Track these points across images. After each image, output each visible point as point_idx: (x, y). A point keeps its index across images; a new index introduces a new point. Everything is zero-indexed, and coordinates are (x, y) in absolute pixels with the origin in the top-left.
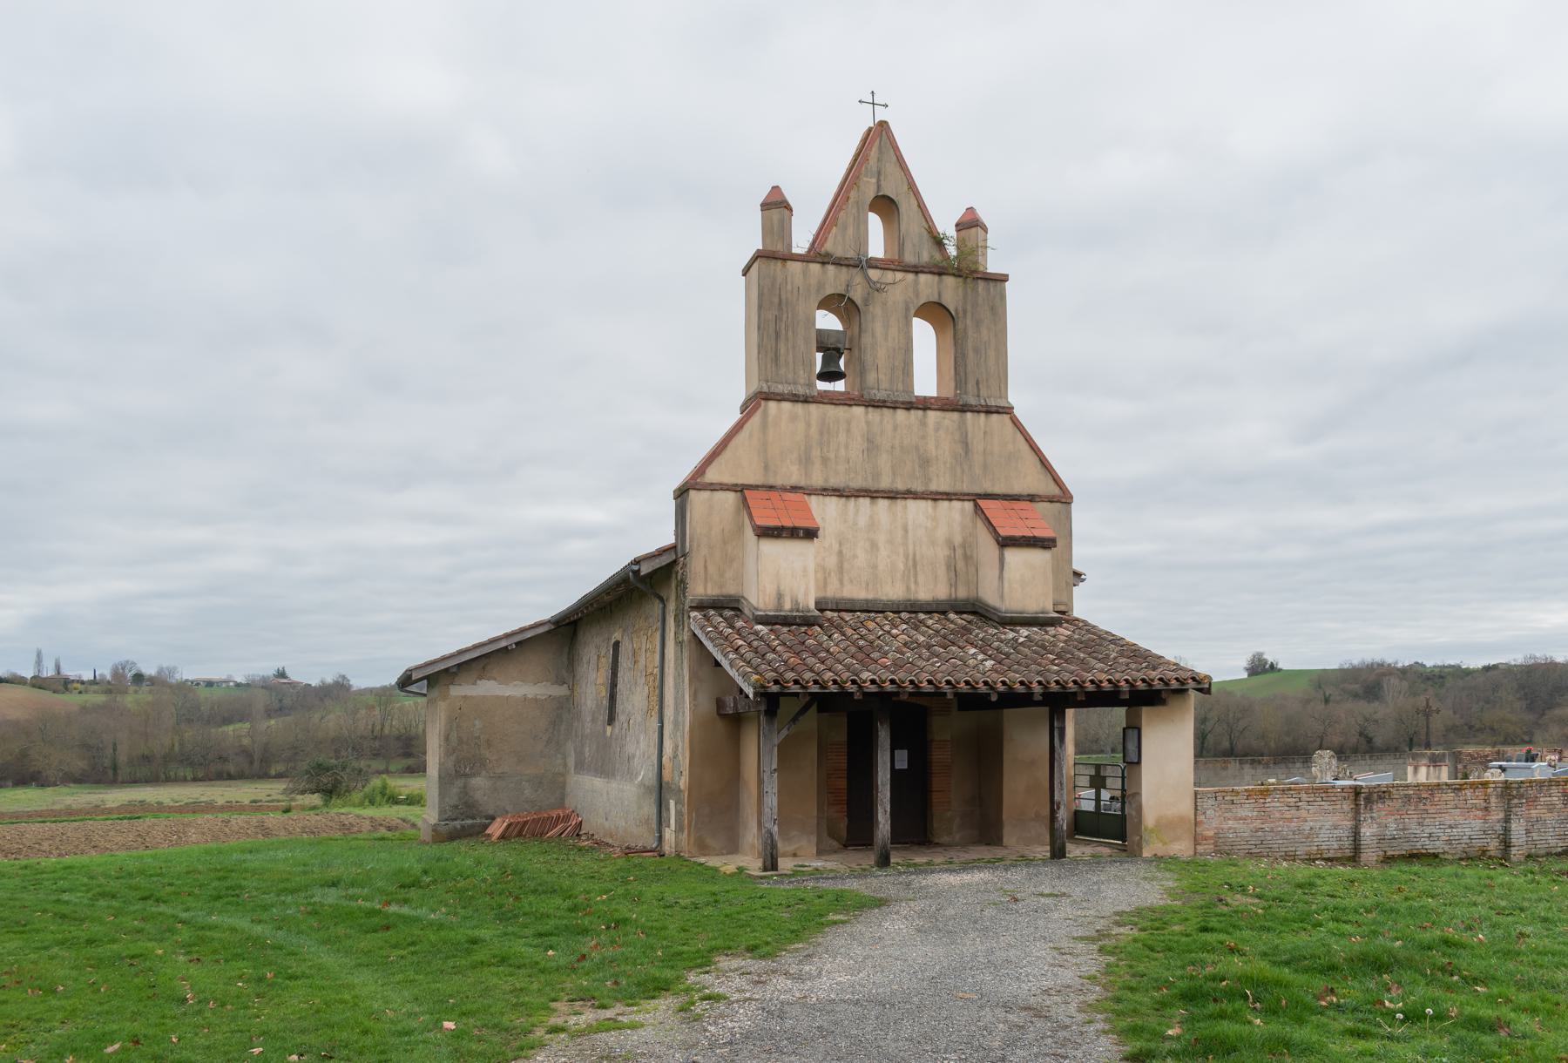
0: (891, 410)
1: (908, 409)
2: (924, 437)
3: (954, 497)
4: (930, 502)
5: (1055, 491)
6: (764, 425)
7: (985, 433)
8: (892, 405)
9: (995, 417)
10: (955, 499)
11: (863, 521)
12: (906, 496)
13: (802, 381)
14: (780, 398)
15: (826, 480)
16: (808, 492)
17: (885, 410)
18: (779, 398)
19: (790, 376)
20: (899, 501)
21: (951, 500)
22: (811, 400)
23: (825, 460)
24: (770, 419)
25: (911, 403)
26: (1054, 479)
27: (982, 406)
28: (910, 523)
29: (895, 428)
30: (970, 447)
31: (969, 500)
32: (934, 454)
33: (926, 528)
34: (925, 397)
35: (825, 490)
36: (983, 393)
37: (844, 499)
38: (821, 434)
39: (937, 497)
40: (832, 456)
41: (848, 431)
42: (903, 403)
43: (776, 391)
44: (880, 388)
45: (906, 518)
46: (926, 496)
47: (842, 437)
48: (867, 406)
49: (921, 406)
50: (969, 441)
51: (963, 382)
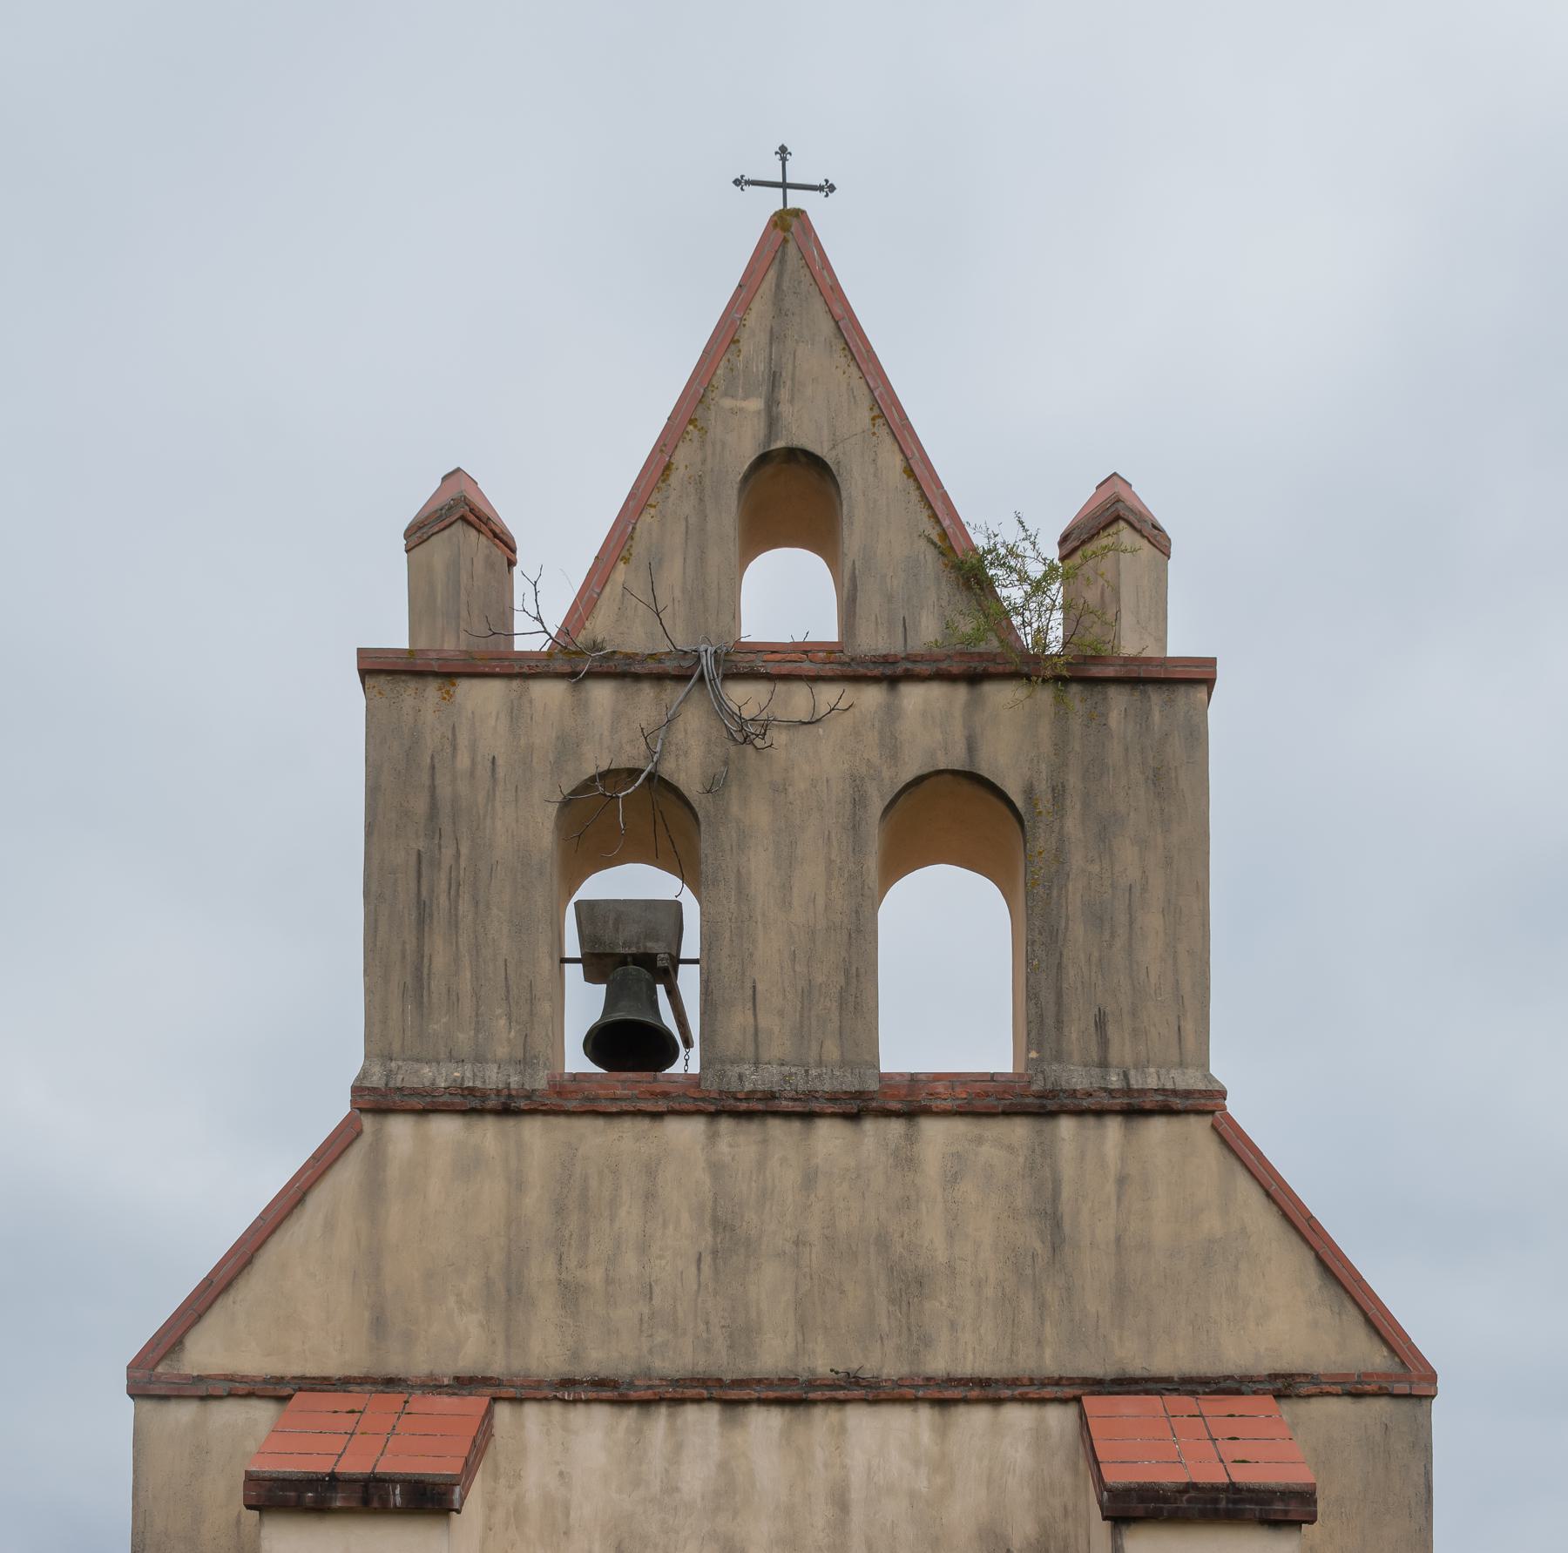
0: (796, 1125)
1: (854, 1117)
2: (906, 1204)
3: (1007, 1393)
4: (925, 1414)
5: (1376, 1359)
6: (374, 1189)
7: (1122, 1180)
8: (798, 1107)
9: (1158, 1127)
10: (1013, 1400)
11: (695, 1477)
12: (840, 1394)
13: (502, 1051)
14: (426, 1105)
15: (576, 1356)
16: (511, 1392)
17: (776, 1127)
18: (417, 1103)
19: (464, 1038)
20: (818, 1412)
21: (997, 1402)
22: (523, 1104)
23: (571, 1294)
24: (393, 1172)
25: (859, 1095)
26: (1370, 1323)
27: (1110, 1092)
28: (856, 1479)
29: (809, 1180)
30: (1067, 1228)
31: (1064, 1401)
32: (942, 1256)
33: (913, 1495)
34: (914, 1078)
35: (567, 1383)
36: (1121, 1049)
37: (632, 1413)
38: (560, 1211)
39: (948, 1394)
40: (595, 1276)
41: (650, 1197)
42: (833, 1098)
43: (413, 1082)
44: (765, 1056)
45: (844, 1467)
46: (909, 1393)
47: (629, 1217)
48: (714, 1115)
49: (894, 1105)
50: (1065, 1208)
51: (1050, 1021)
